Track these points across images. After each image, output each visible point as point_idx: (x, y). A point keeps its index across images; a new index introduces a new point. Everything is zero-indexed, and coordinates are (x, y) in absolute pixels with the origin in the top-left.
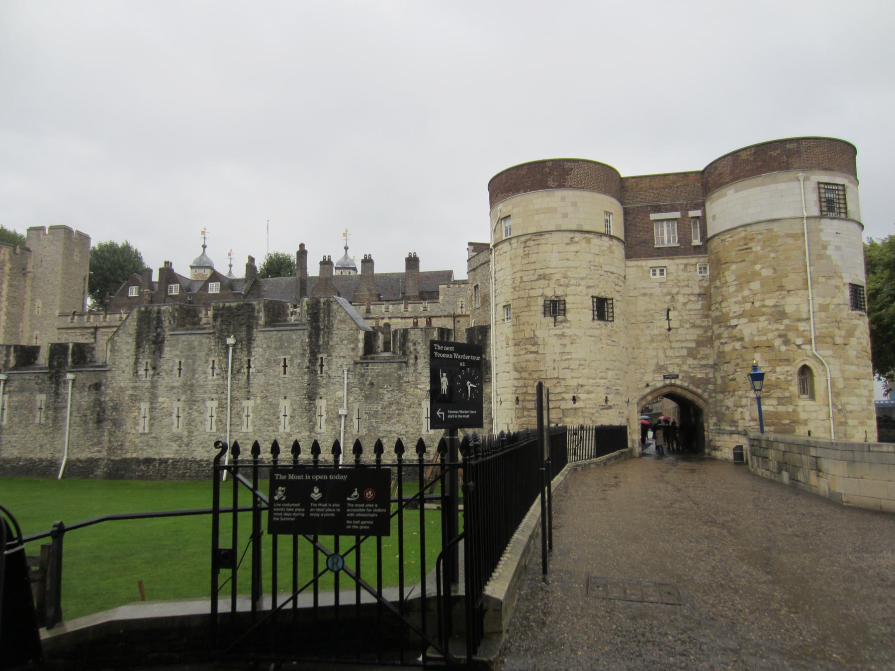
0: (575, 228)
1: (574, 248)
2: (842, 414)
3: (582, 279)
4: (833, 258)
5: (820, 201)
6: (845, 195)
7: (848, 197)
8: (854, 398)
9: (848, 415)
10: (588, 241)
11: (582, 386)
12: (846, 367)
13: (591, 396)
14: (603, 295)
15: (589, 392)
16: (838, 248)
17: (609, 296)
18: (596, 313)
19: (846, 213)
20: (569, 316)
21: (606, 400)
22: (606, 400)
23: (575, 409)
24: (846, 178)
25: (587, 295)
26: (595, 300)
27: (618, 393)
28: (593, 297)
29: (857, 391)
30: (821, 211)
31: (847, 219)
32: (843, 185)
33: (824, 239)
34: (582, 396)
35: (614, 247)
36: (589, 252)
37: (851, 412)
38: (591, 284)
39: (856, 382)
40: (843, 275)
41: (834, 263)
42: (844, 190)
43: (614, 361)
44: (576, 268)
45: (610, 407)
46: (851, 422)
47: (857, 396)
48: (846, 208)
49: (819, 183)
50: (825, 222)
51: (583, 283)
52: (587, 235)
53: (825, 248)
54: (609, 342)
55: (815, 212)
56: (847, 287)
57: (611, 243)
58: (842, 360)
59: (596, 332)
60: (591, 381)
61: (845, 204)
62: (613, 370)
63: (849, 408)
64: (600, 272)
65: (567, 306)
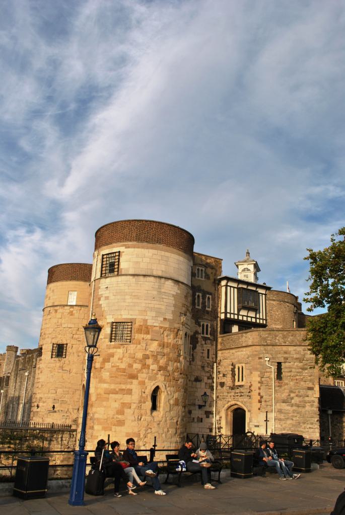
0: (51, 305)
1: (49, 317)
2: (92, 421)
3: (50, 334)
4: (102, 306)
5: (102, 267)
6: (119, 259)
7: (121, 259)
8: (103, 409)
9: (95, 421)
10: (56, 311)
11: (42, 398)
12: (99, 384)
13: (45, 404)
14: (60, 342)
15: (44, 402)
16: (107, 298)
17: (65, 342)
18: (54, 353)
19: (118, 271)
20: (43, 357)
21: (54, 407)
22: (54, 407)
23: (37, 412)
24: (122, 246)
25: (51, 343)
26: (55, 345)
27: (63, 402)
28: (53, 344)
29: (105, 403)
30: (102, 274)
31: (118, 275)
32: (119, 252)
33: (100, 293)
34: (41, 404)
35: (74, 312)
36: (56, 318)
37: (98, 419)
38: (53, 337)
39: (106, 396)
40: (107, 317)
41: (103, 309)
42: (119, 256)
43: (63, 383)
44: (49, 328)
45: (55, 412)
46: (96, 427)
47: (105, 407)
48: (118, 268)
49: (103, 255)
50: (103, 280)
51: (50, 336)
52: (56, 308)
53: (99, 299)
54: (61, 371)
55: (98, 276)
56: (109, 325)
57: (72, 309)
58: (98, 379)
59: (52, 365)
60: (46, 395)
61: (118, 265)
62: (61, 388)
63: (96, 416)
64: (61, 328)
65: (43, 351)
